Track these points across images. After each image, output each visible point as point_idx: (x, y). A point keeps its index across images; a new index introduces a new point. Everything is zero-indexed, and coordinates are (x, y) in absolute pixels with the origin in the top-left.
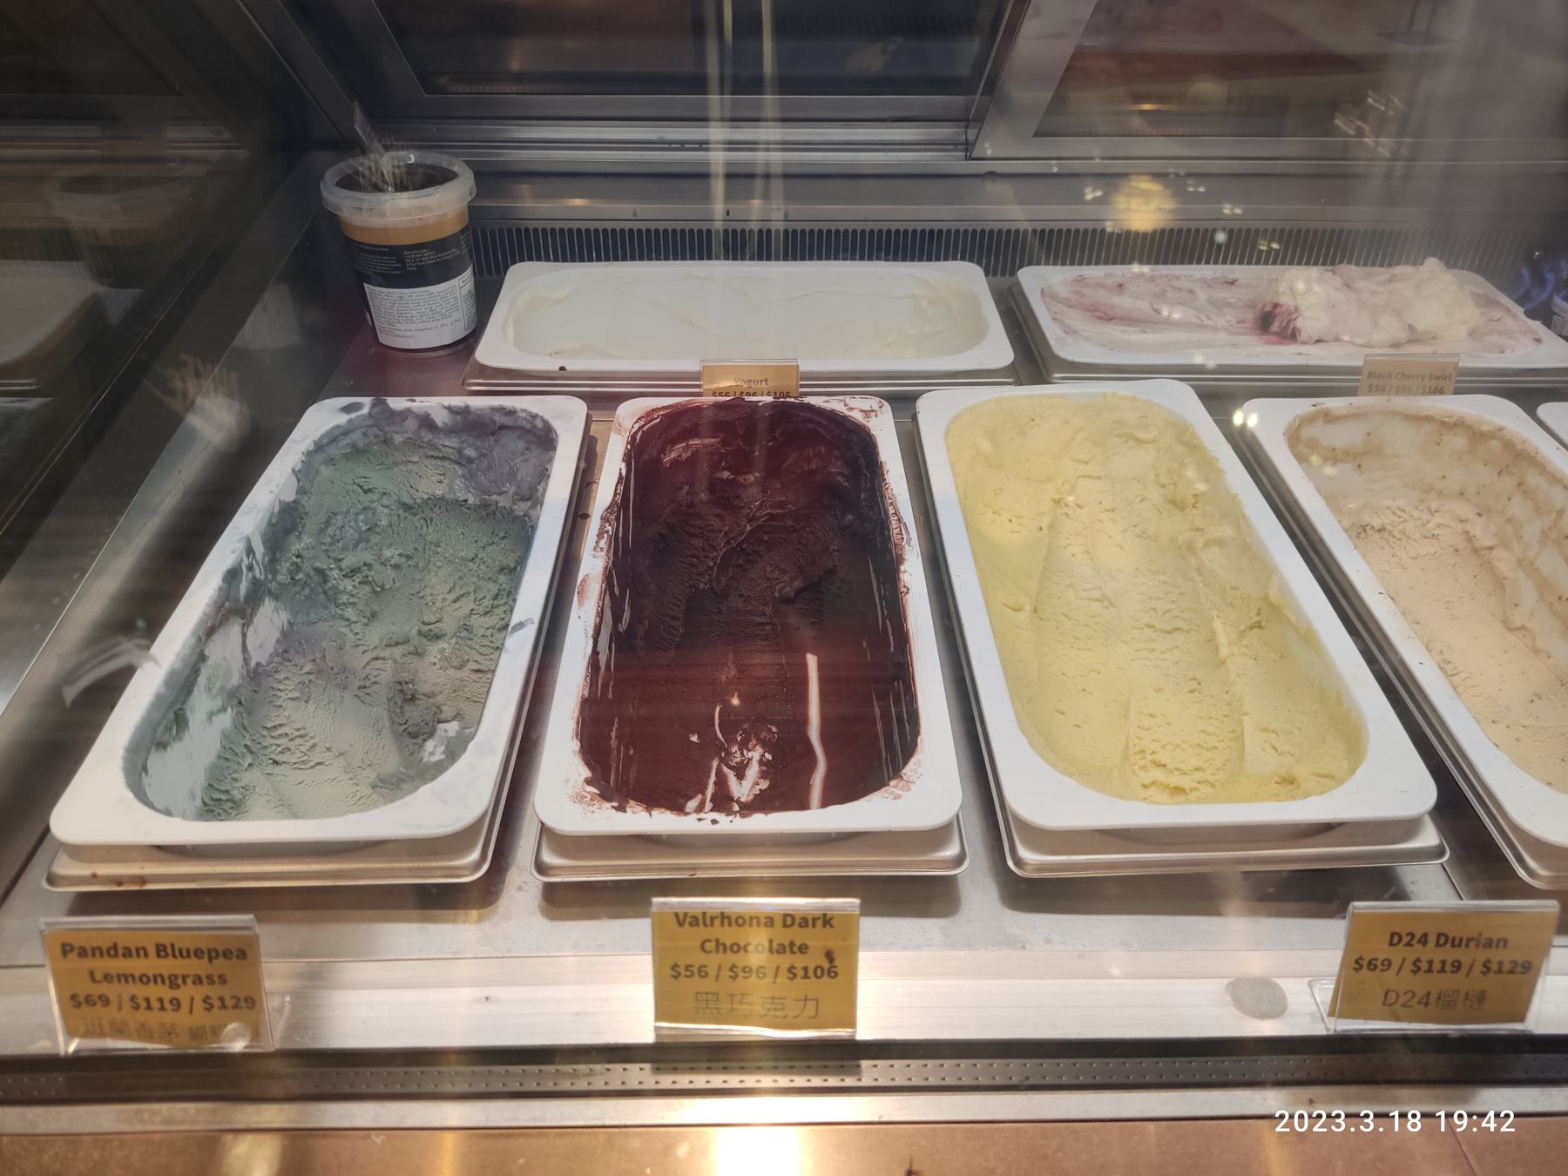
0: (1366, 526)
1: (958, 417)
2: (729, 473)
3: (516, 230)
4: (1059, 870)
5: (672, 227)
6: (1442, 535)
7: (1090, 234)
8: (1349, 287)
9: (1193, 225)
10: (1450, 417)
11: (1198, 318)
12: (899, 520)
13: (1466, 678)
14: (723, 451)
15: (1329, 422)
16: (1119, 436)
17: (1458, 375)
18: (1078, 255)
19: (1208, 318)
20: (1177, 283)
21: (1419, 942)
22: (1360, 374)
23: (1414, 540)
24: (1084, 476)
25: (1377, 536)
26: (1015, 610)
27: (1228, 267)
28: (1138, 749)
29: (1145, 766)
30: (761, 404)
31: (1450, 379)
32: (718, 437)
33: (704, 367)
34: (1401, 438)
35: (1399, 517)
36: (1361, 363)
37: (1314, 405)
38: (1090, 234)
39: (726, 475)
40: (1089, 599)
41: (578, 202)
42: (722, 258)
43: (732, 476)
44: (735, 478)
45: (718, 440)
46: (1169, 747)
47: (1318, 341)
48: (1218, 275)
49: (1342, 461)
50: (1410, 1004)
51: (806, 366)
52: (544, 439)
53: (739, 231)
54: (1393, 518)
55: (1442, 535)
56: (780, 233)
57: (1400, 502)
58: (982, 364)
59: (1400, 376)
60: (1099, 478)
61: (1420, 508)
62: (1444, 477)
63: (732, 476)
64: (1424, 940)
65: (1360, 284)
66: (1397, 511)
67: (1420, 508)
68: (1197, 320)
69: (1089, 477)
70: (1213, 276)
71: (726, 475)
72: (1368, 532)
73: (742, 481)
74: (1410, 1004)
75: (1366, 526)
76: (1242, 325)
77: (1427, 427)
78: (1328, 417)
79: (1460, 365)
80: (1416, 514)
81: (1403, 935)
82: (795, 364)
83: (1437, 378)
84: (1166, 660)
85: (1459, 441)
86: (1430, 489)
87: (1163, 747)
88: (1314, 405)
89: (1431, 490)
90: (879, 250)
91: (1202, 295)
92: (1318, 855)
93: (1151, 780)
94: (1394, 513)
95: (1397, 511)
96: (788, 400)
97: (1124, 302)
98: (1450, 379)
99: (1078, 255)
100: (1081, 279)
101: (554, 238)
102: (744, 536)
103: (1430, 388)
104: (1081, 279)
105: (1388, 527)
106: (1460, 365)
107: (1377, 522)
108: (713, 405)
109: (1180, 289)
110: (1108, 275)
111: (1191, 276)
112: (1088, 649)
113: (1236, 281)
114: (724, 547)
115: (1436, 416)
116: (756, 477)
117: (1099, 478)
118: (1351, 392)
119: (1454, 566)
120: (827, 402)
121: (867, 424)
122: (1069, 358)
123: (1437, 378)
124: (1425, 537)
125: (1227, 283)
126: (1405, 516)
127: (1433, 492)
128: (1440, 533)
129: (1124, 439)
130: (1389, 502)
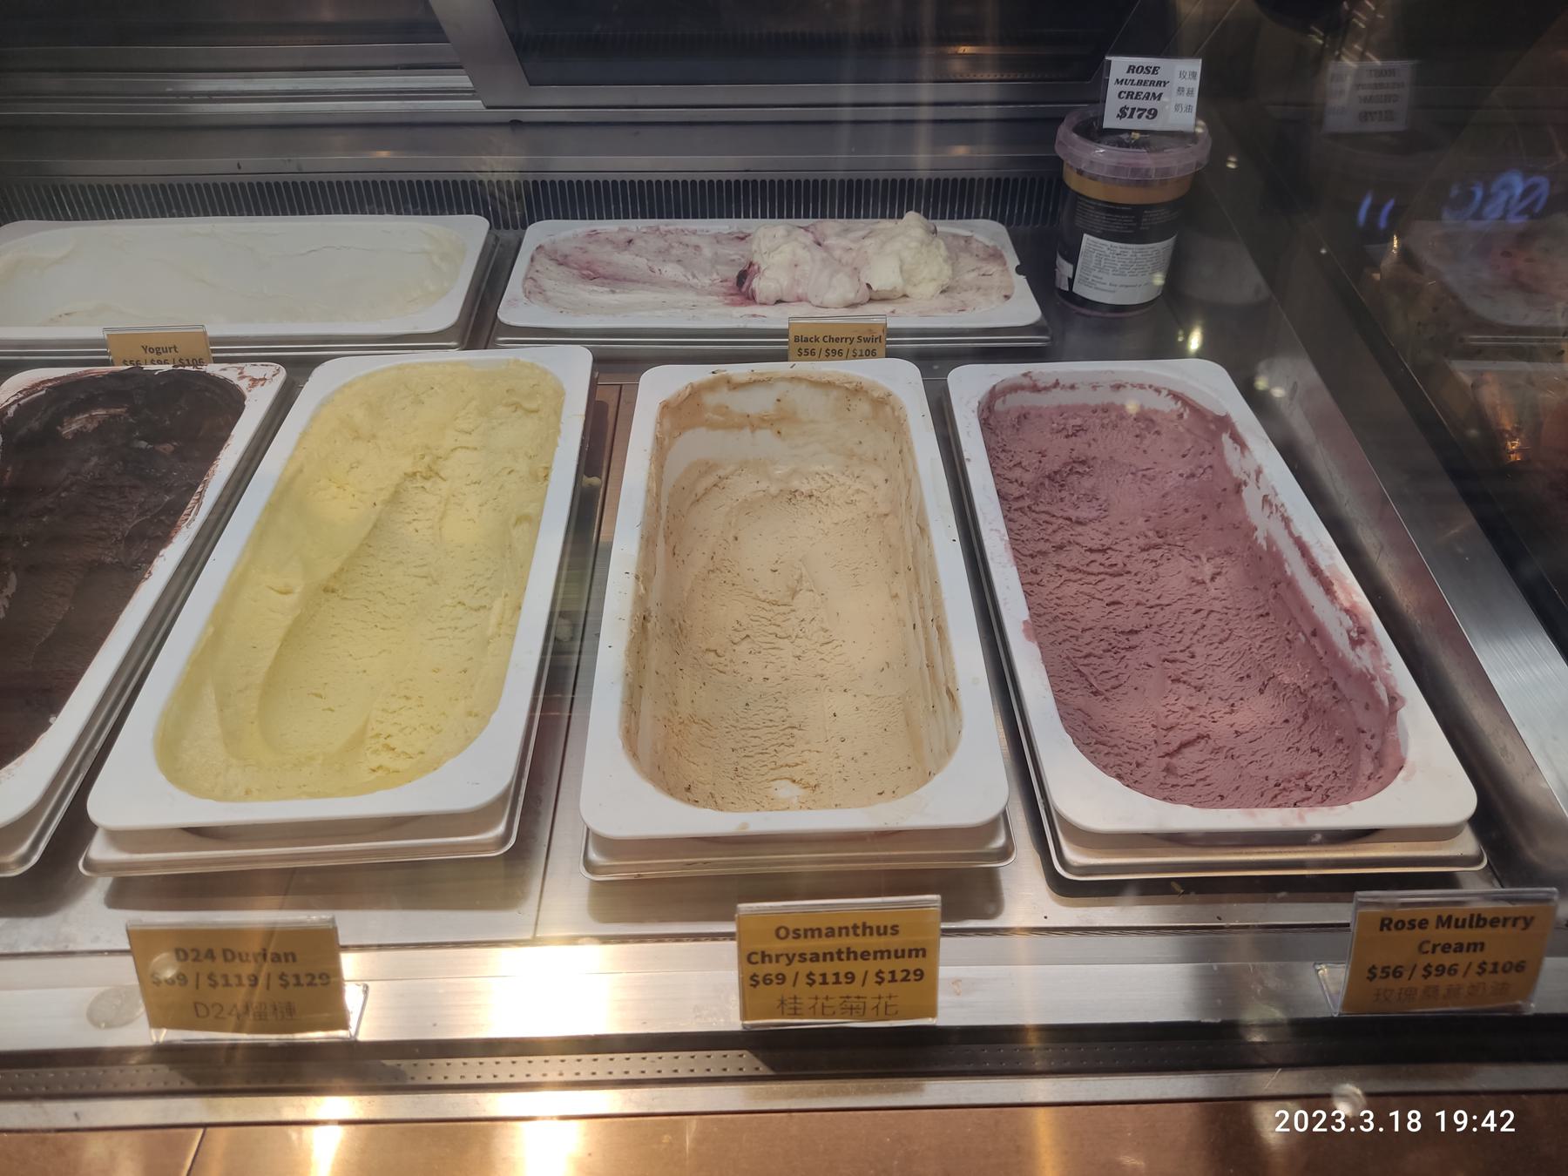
0: (796, 491)
1: (349, 385)
2: (146, 444)
3: (240, 184)
4: (309, 859)
5: (595, 179)
6: (859, 501)
7: (1002, 183)
8: (819, 244)
9: (942, 175)
10: (850, 383)
11: (685, 276)
12: (198, 500)
13: (1064, 641)
14: (131, 420)
15: (735, 388)
16: (507, 405)
17: (889, 336)
18: (613, 207)
19: (694, 276)
20: (685, 239)
21: (206, 957)
22: (787, 336)
23: (838, 506)
24: (461, 447)
25: (808, 501)
26: (281, 593)
27: (743, 221)
28: (374, 733)
29: (377, 750)
30: (156, 373)
31: (880, 341)
32: (123, 407)
33: (108, 335)
34: (803, 399)
35: (828, 483)
36: (787, 326)
37: (713, 373)
38: (1002, 183)
39: (143, 444)
40: (416, 576)
41: (384, 154)
42: (211, 214)
43: (150, 446)
44: (154, 448)
45: (123, 410)
46: (408, 731)
47: (779, 302)
48: (735, 229)
49: (760, 428)
50: (221, 1016)
51: (213, 331)
52: (230, 402)
53: (557, 182)
54: (820, 483)
55: (859, 501)
56: (529, 184)
57: (828, 468)
58: (417, 328)
59: (827, 339)
60: (476, 449)
61: (847, 473)
62: (860, 443)
63: (150, 446)
64: (210, 954)
65: (831, 242)
66: (825, 476)
67: (847, 473)
68: (683, 278)
69: (465, 447)
70: (729, 231)
71: (143, 444)
72: (798, 497)
73: (161, 450)
74: (221, 1016)
75: (796, 491)
76: (725, 284)
77: (834, 393)
78: (733, 385)
79: (888, 326)
80: (842, 479)
81: (189, 952)
82: (201, 330)
83: (867, 340)
84: (463, 638)
85: (863, 407)
86: (851, 455)
87: (402, 730)
88: (713, 373)
89: (854, 456)
90: (405, 202)
91: (707, 252)
92: (169, 861)
93: (378, 764)
94: (823, 478)
95: (825, 476)
96: (187, 368)
97: (625, 259)
98: (880, 341)
99: (613, 207)
100: (593, 234)
101: (350, 191)
102: (161, 508)
103: (861, 351)
104: (593, 234)
105: (815, 493)
106: (888, 326)
107: (805, 488)
108: (107, 375)
109: (687, 245)
110: (622, 230)
111: (707, 231)
112: (393, 628)
113: (749, 235)
114: (136, 519)
115: (837, 383)
116: (175, 446)
117: (476, 449)
118: (782, 357)
119: (866, 532)
120: (225, 370)
121: (246, 393)
122: (513, 323)
123: (867, 340)
124: (847, 503)
125: (738, 238)
126: (831, 480)
127: (855, 458)
128: (858, 499)
129: (513, 408)
130: (818, 468)
